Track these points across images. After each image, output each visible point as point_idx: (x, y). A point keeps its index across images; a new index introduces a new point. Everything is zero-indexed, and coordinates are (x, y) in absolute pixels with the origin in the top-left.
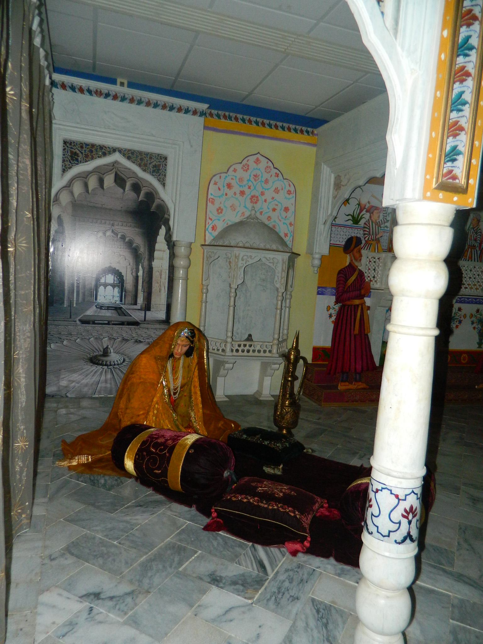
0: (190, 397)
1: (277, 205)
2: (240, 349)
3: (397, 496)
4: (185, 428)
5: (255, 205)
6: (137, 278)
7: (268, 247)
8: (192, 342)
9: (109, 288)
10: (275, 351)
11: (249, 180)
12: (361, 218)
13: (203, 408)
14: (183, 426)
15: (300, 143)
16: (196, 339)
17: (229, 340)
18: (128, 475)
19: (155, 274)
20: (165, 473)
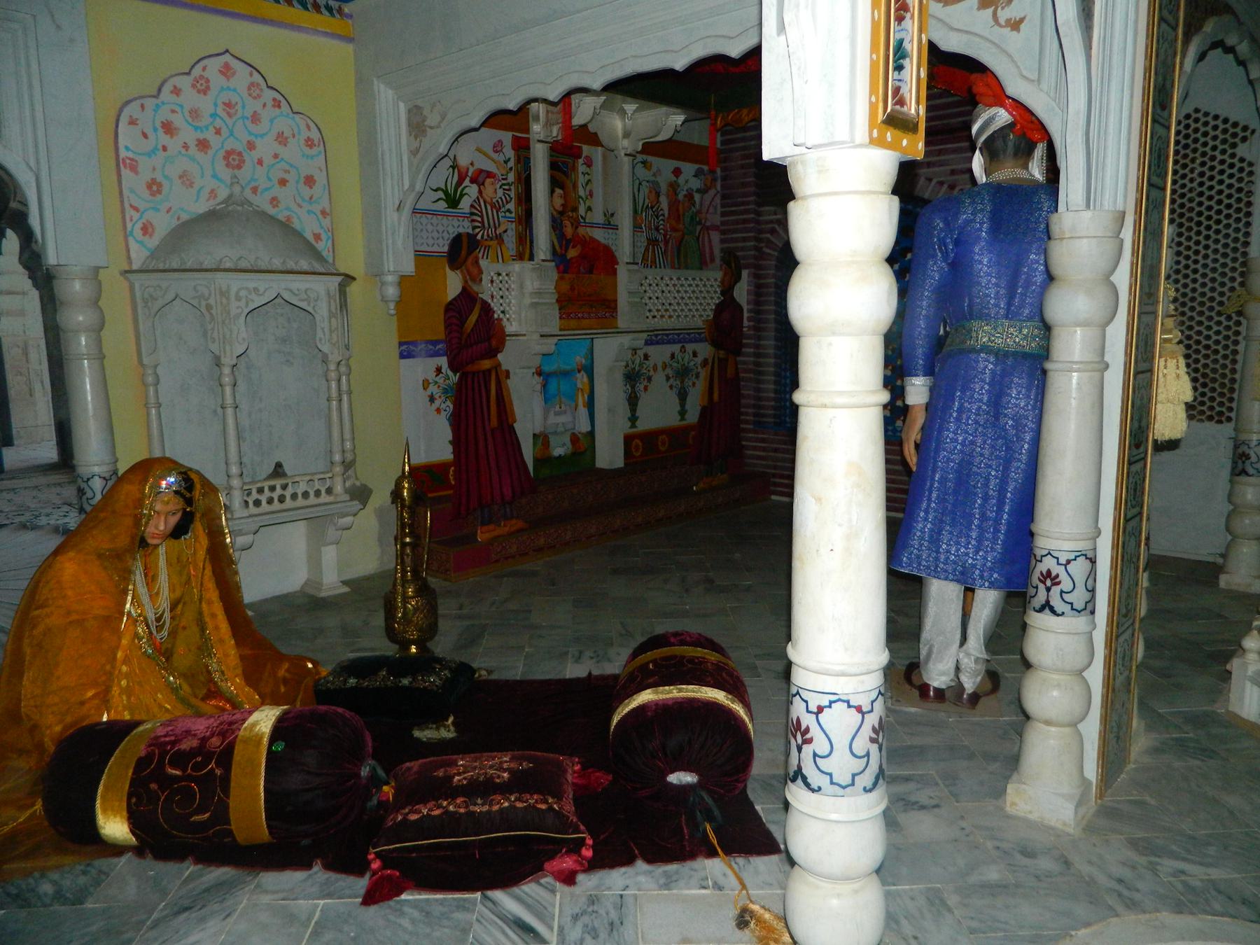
0: (203, 628)
1: (287, 172)
2: (264, 499)
3: (859, 709)
4: (203, 699)
5: (236, 171)
7: (291, 265)
8: (189, 502)
10: (338, 488)
11: (214, 115)
12: (462, 195)
13: (238, 644)
14: (196, 697)
15: (316, 32)
16: (197, 493)
17: (236, 482)
18: (116, 849)
20: (222, 814)
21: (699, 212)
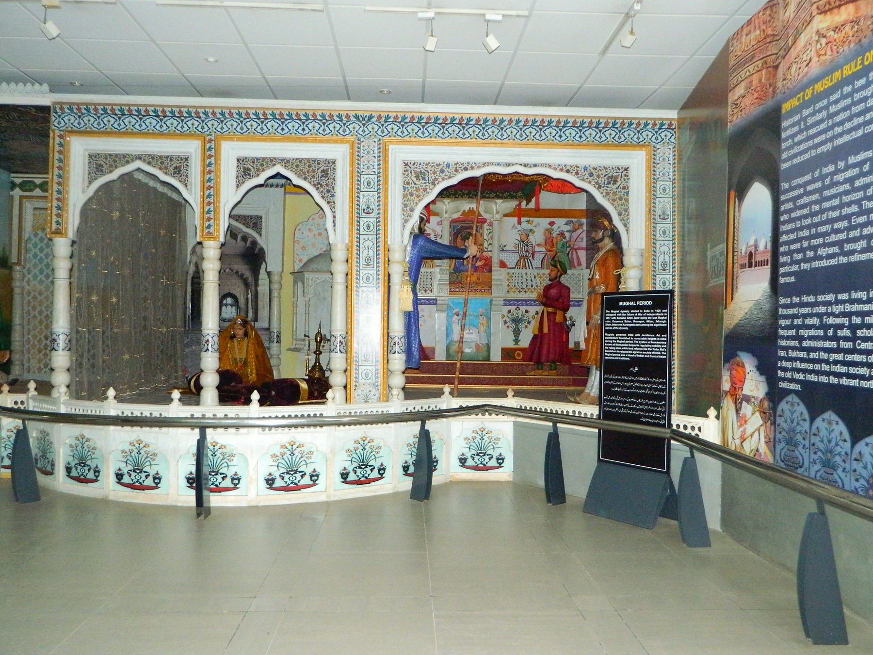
6: (247, 299)
9: (229, 307)
19: (260, 296)
21: (570, 241)
